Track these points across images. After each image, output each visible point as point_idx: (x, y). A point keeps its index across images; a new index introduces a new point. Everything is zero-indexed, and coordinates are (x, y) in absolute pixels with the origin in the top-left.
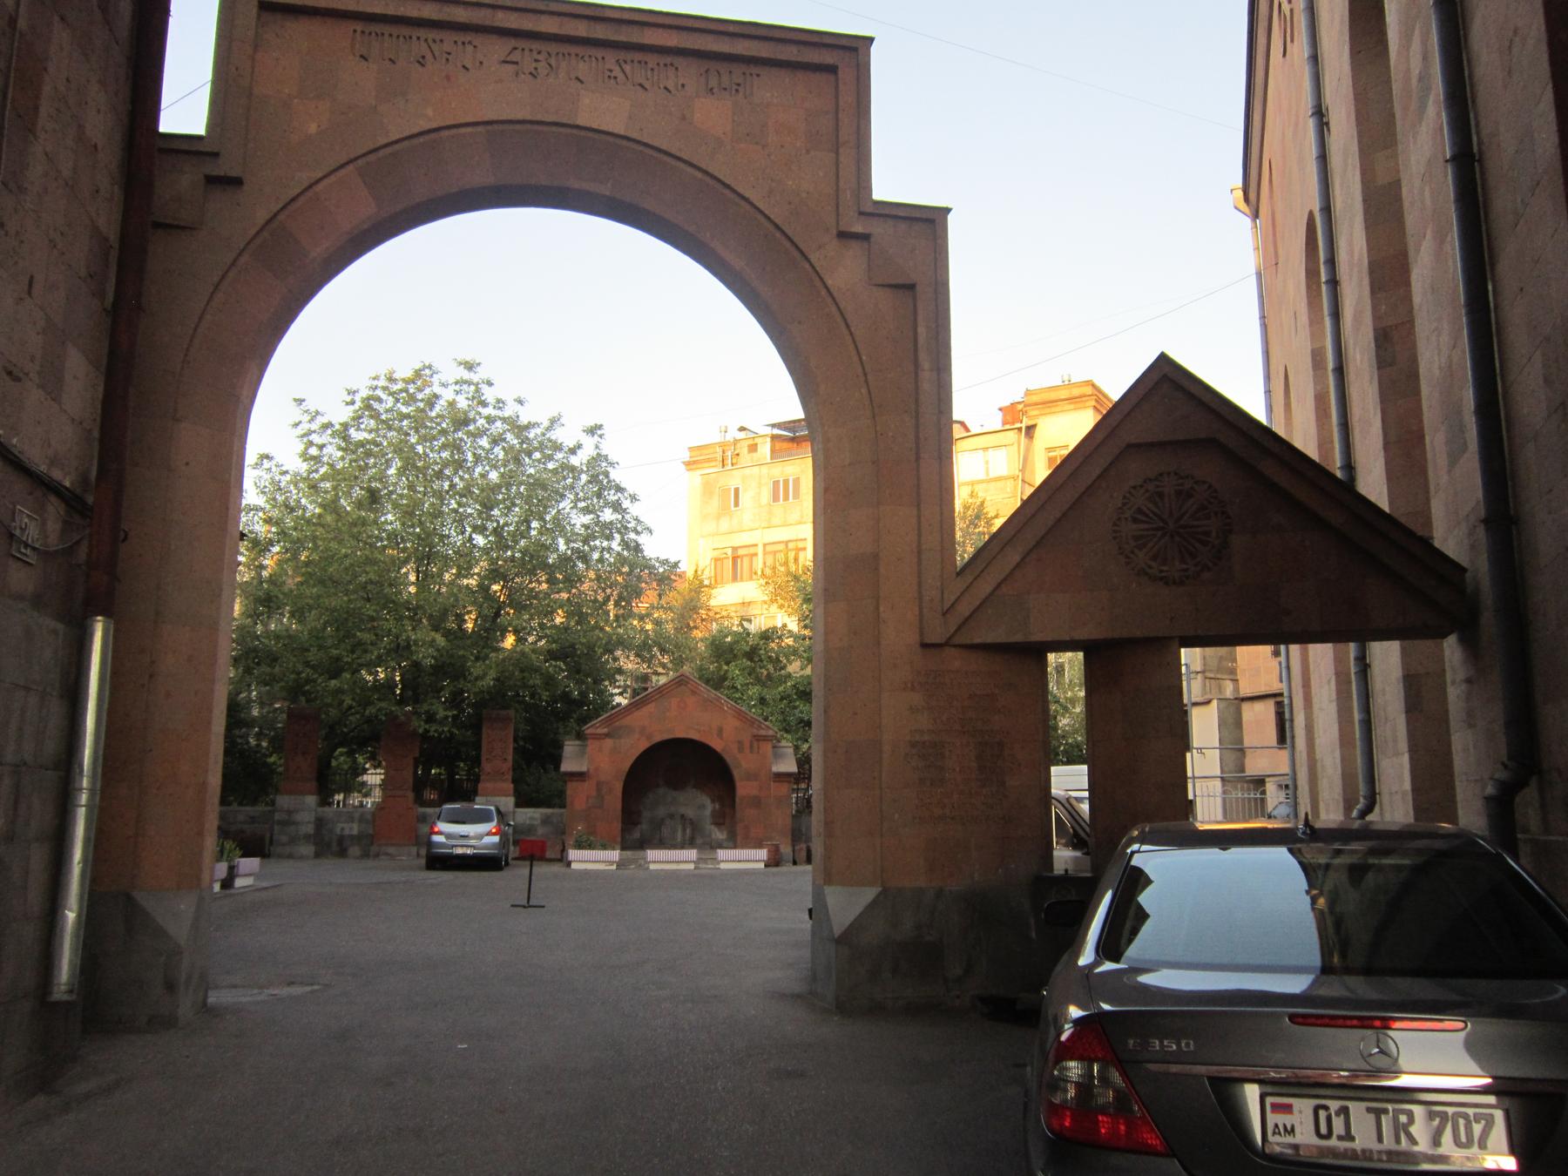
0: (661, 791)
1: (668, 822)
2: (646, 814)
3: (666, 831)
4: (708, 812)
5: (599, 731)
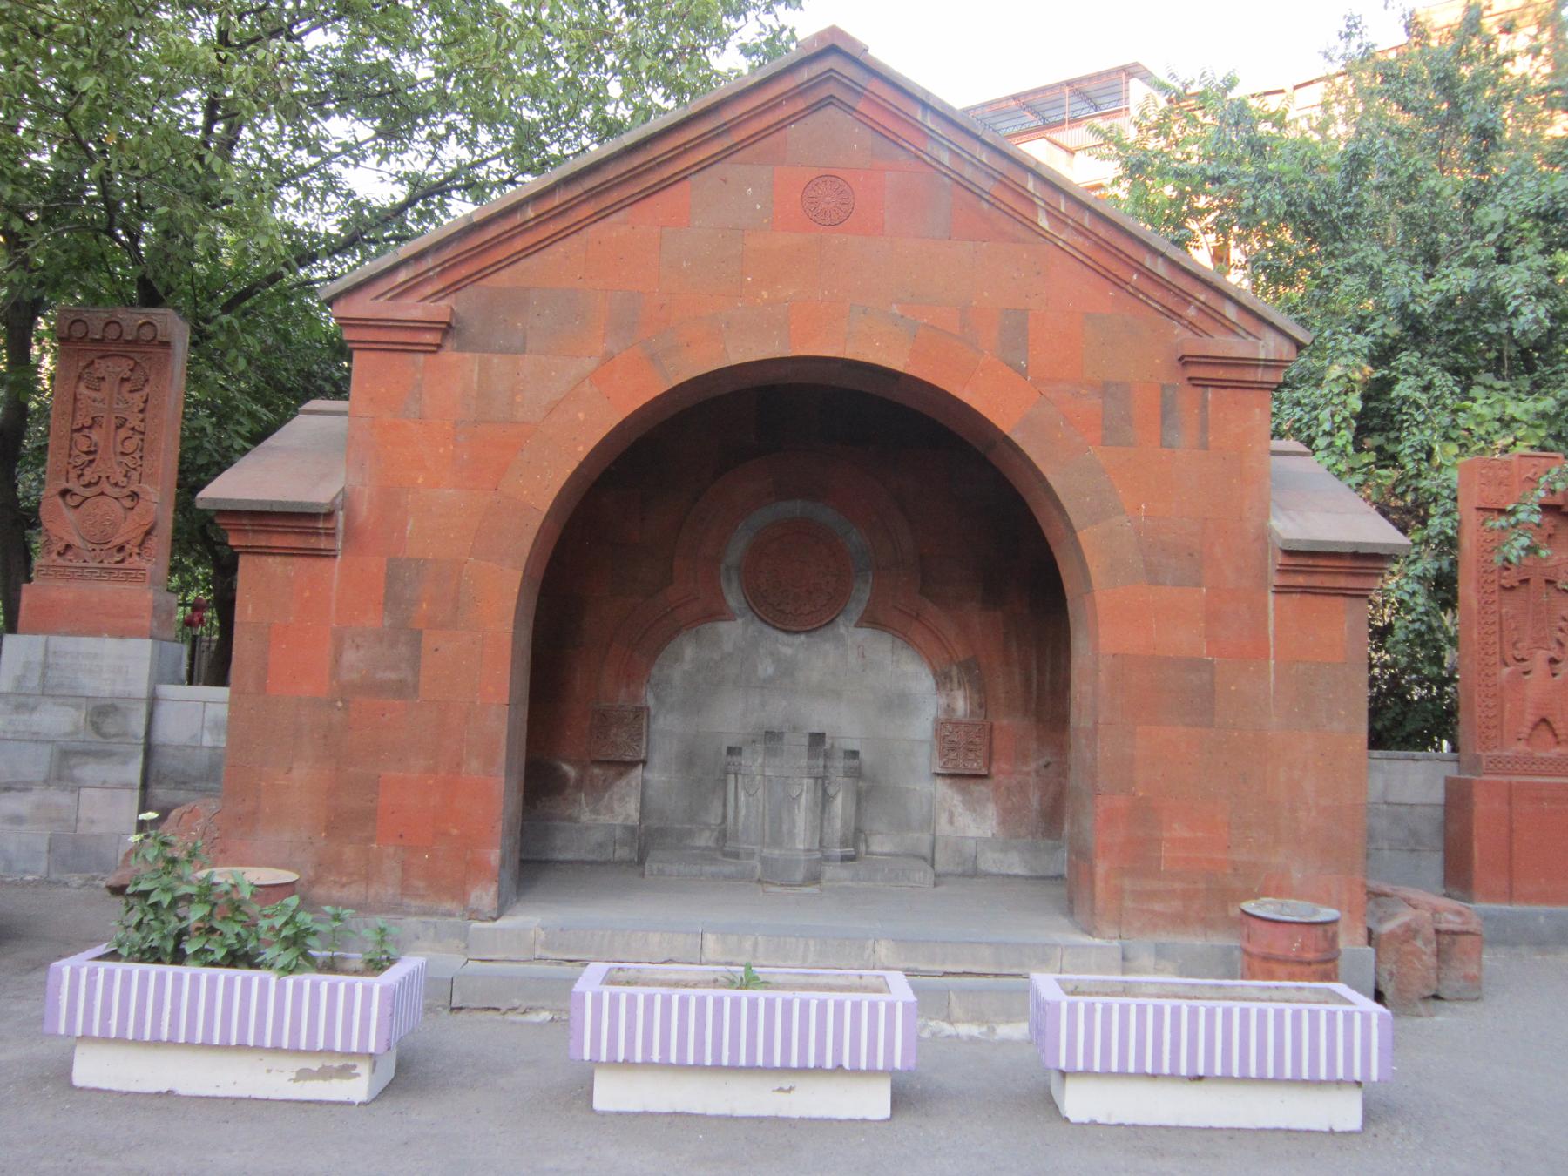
0: (734, 632)
1: (753, 762)
2: (668, 728)
3: (745, 804)
4: (922, 726)
5: (412, 309)
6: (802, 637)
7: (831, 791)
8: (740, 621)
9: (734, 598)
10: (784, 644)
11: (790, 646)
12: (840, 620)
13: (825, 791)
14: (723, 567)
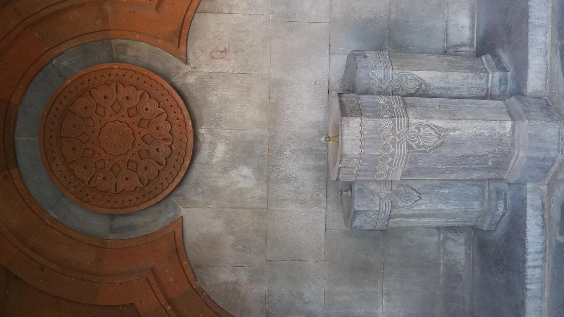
0: (199, 218)
6: (202, 131)
7: (411, 87)
8: (183, 212)
9: (149, 222)
10: (212, 155)
11: (215, 150)
12: (178, 81)
13: (411, 95)
14: (112, 237)
